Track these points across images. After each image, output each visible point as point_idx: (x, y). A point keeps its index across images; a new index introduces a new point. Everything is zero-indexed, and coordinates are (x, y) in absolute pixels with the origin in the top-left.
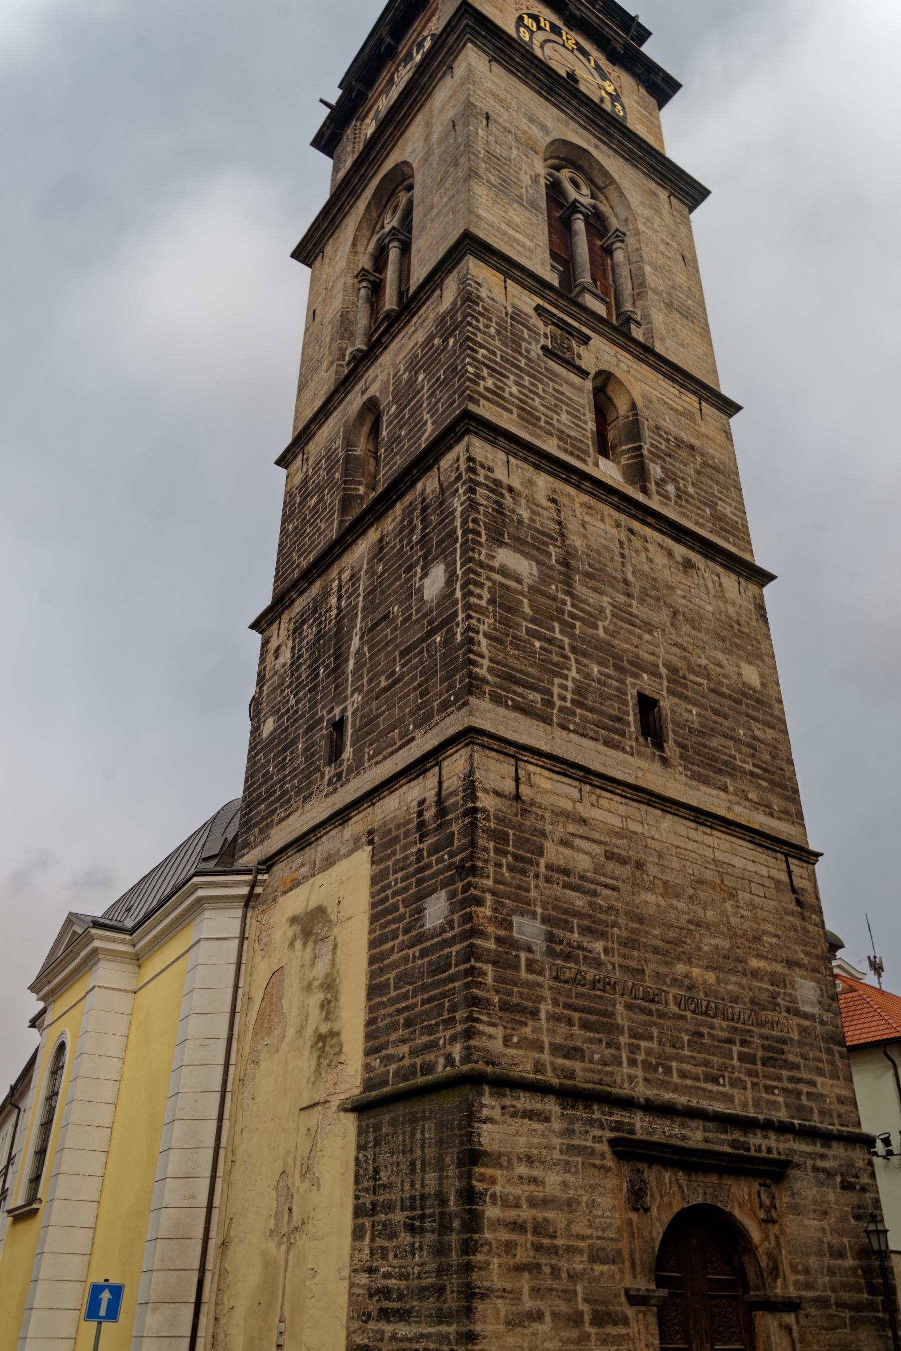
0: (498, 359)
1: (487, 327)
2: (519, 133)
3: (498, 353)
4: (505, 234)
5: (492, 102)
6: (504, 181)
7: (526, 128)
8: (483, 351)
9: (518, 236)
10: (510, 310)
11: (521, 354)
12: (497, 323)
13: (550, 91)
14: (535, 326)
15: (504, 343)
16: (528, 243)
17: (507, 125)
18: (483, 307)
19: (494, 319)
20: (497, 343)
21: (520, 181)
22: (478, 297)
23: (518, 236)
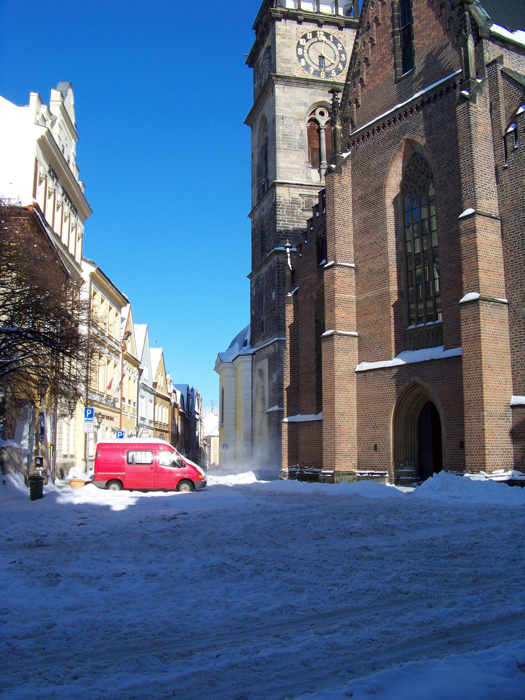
0: (287, 222)
1: (283, 212)
2: (295, 116)
3: (287, 220)
4: (289, 168)
5: (284, 109)
6: (289, 144)
7: (298, 111)
8: (282, 222)
9: (294, 166)
10: (290, 200)
11: (294, 216)
12: (286, 209)
13: (307, 84)
14: (300, 201)
15: (288, 215)
16: (297, 166)
17: (291, 115)
18: (282, 205)
19: (285, 207)
20: (286, 216)
21: (295, 139)
22: (280, 202)
23: (294, 166)
